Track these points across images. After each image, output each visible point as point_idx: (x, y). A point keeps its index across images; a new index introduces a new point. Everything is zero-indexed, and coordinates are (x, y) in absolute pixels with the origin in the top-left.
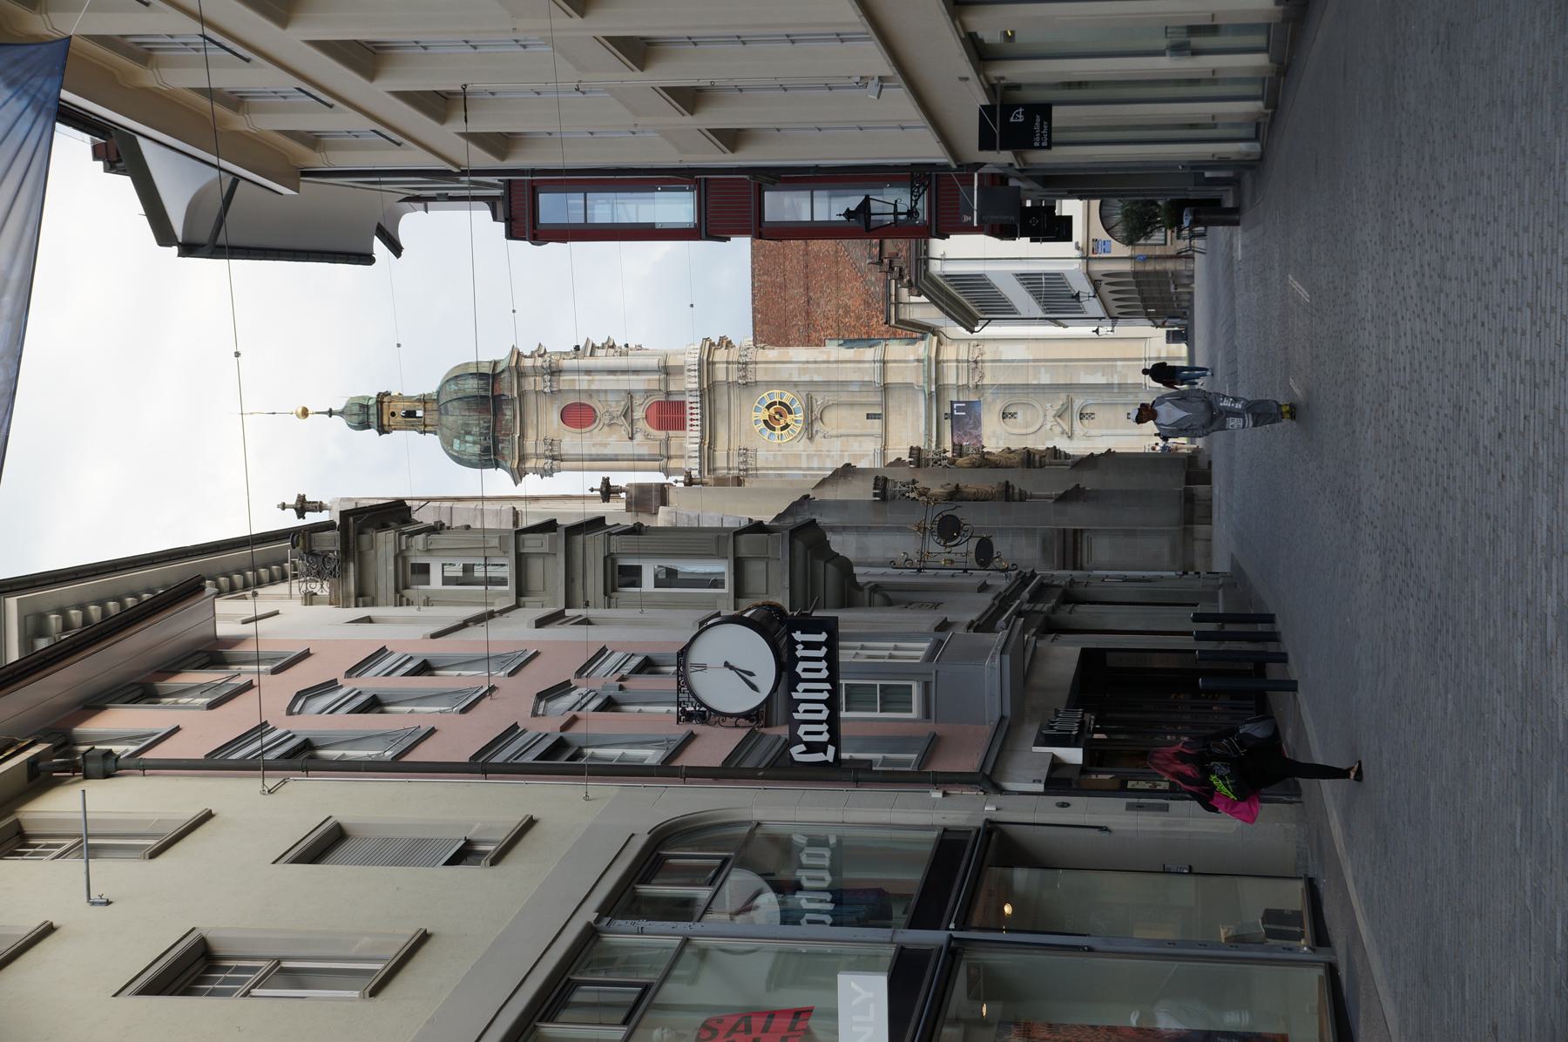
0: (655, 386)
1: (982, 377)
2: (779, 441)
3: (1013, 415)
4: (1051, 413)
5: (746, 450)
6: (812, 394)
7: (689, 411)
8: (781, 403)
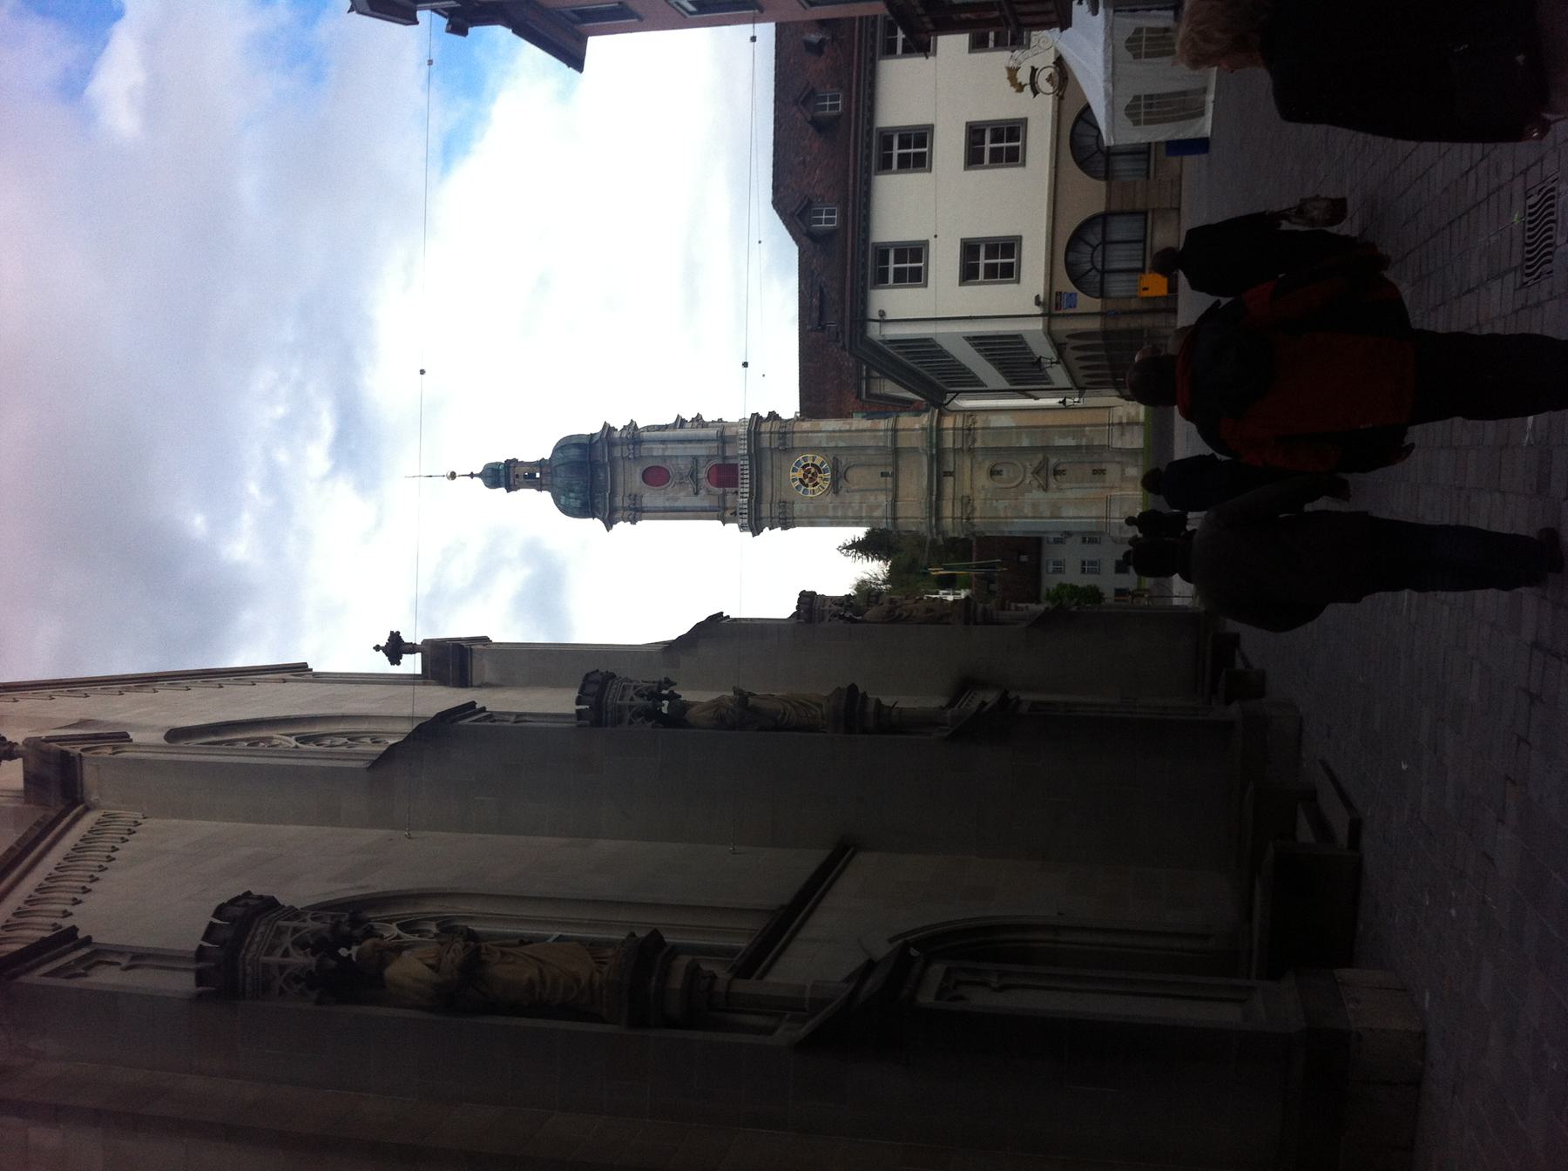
0: (714, 452)
1: (974, 441)
2: (811, 496)
3: (999, 473)
4: (1030, 469)
5: (784, 502)
6: (839, 458)
7: (740, 472)
8: (813, 465)
